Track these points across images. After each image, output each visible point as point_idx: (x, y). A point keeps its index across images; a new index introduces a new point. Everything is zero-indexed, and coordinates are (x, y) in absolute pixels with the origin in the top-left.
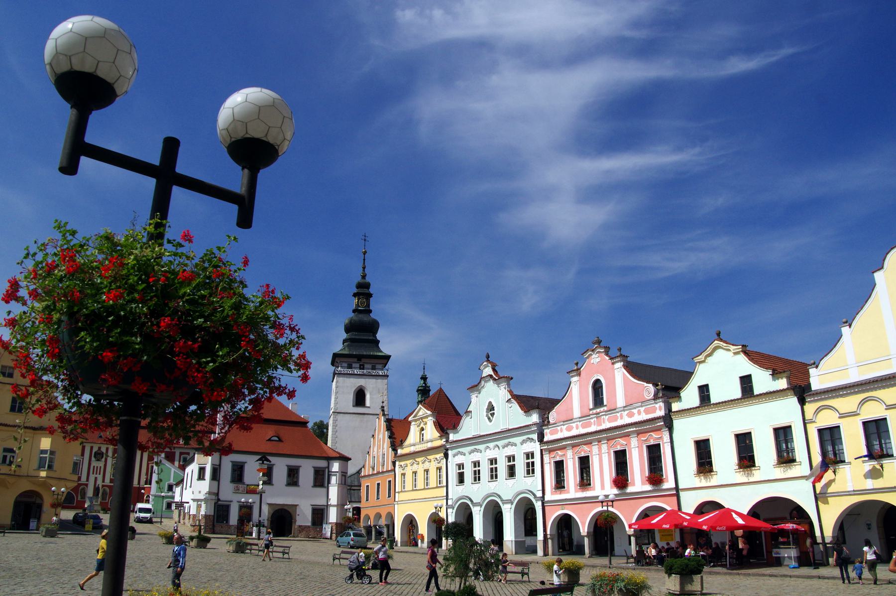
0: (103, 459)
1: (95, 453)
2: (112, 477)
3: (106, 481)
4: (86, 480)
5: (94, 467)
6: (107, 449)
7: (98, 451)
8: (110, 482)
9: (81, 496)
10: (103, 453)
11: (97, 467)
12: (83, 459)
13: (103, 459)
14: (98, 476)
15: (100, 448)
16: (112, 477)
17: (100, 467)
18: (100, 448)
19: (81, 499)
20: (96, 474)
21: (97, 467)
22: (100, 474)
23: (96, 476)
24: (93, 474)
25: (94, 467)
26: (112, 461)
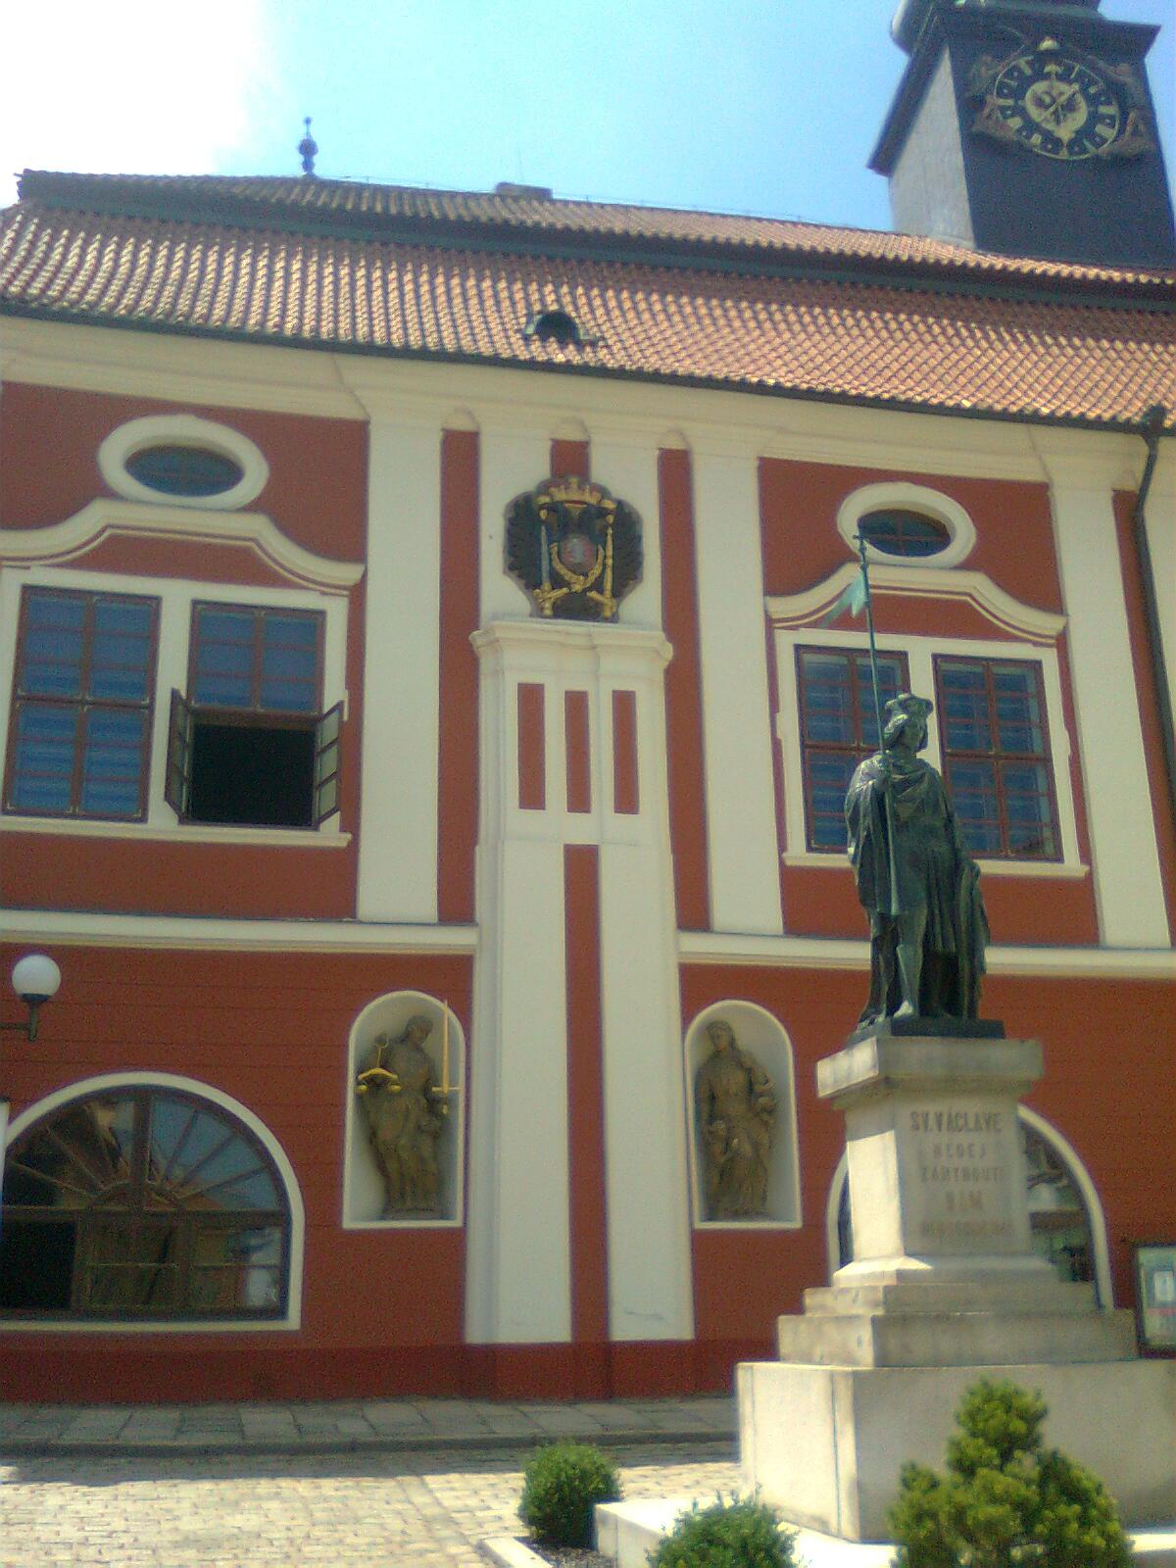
0: (646, 598)
1: (523, 516)
2: (798, 853)
3: (723, 910)
4: (427, 904)
5: (531, 698)
6: (675, 470)
7: (544, 488)
8: (797, 924)
9: (380, 1156)
10: (626, 523)
11: (576, 704)
12: (357, 596)
13: (646, 598)
14: (599, 826)
15: (570, 459)
16: (798, 853)
17: (624, 704)
18: (570, 459)
19: (388, 1210)
20: (579, 799)
21: (576, 704)
22: (627, 800)
23: (581, 830)
24: (532, 795)
25: (531, 698)
26: (770, 623)
